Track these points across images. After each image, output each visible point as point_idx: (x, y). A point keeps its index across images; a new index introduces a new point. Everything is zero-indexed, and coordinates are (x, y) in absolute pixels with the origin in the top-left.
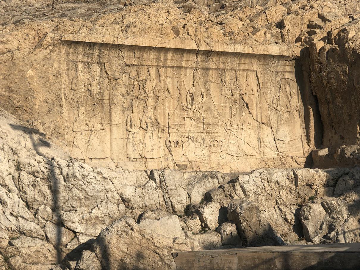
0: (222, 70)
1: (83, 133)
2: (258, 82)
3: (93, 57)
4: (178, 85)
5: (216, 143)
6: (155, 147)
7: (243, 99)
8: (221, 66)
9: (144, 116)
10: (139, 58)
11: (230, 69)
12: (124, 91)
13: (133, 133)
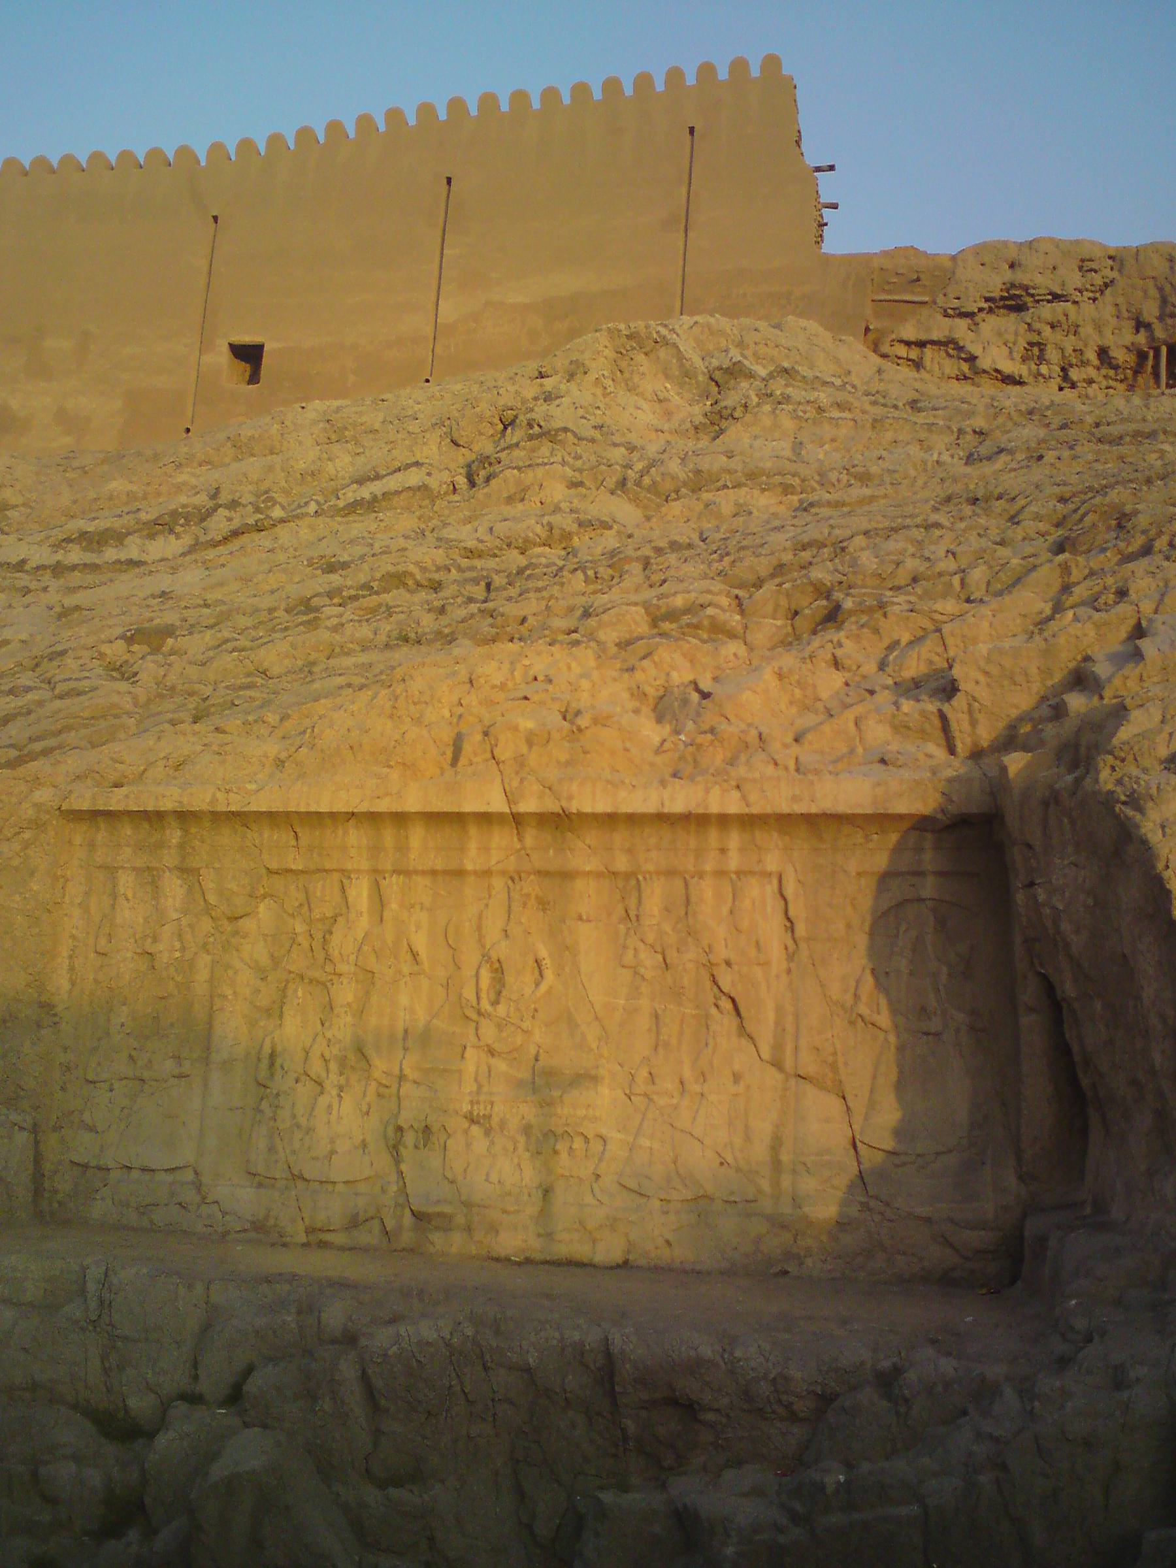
1: (116, 1085)
2: (788, 919)
4: (451, 931)
5: (578, 1143)
7: (715, 982)
8: (622, 863)
9: (320, 1039)
11: (658, 873)
13: (275, 1092)
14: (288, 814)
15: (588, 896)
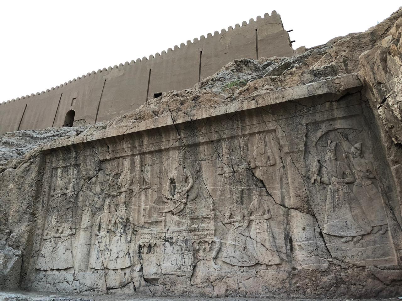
0: (219, 141)
1: (52, 240)
3: (71, 160)
8: (215, 137)
10: (113, 151)
11: (228, 138)
12: (98, 189)
14: (104, 139)
15: (204, 151)
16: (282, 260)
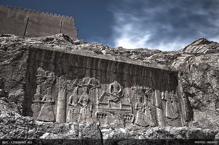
6: (88, 117)
16: (155, 125)
